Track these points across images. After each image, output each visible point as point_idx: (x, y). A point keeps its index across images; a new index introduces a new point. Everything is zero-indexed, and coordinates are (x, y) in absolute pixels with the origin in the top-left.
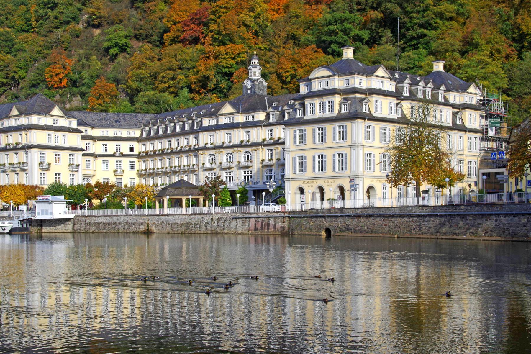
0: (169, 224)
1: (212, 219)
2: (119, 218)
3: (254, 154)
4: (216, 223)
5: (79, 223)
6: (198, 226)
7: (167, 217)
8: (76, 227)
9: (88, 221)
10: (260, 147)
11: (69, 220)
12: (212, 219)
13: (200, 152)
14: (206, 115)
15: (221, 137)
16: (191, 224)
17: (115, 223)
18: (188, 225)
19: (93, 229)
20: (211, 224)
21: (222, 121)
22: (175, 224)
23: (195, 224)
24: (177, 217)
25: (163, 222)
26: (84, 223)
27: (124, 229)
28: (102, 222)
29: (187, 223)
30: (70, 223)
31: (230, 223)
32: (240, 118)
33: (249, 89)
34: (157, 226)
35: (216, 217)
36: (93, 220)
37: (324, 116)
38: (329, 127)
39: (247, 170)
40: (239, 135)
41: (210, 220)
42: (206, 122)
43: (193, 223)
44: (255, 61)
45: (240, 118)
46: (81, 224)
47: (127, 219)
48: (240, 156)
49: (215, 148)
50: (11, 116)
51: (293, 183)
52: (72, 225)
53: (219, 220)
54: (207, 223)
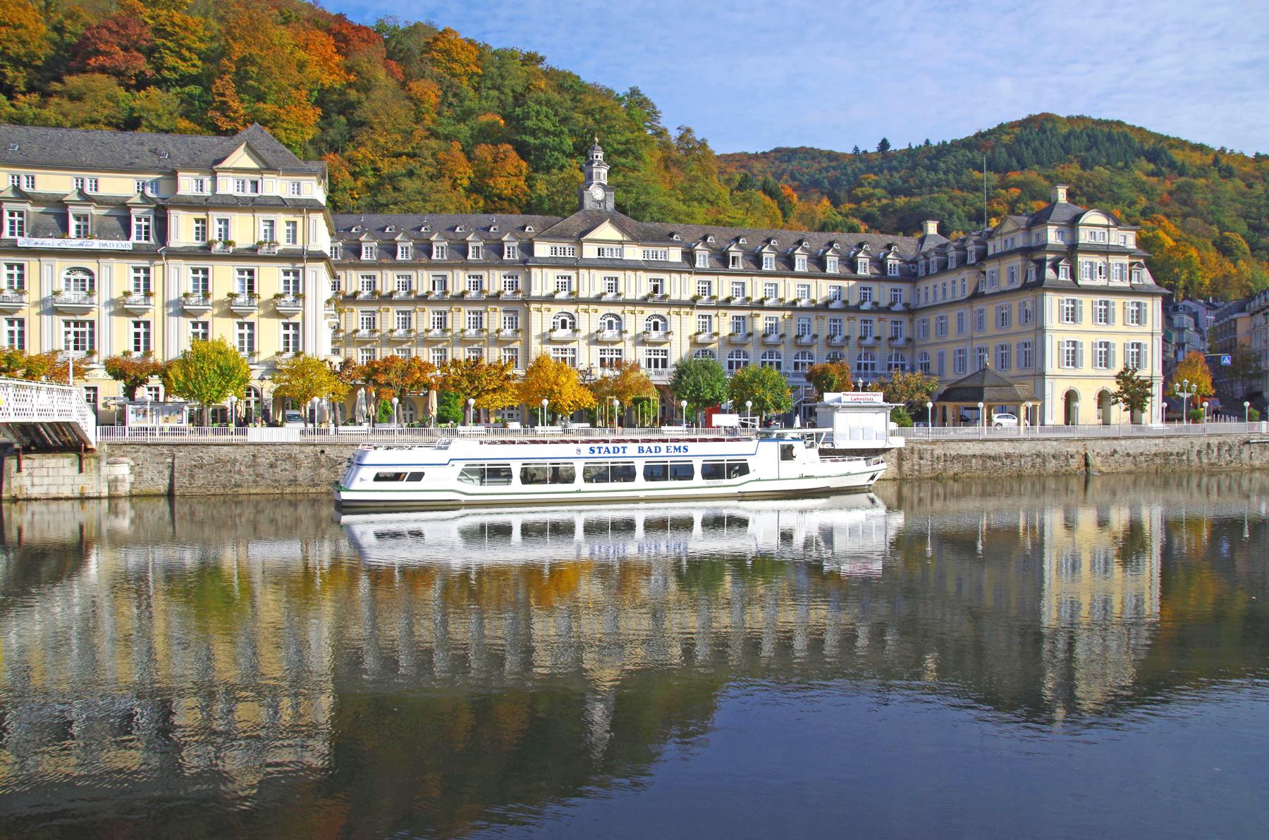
0: (1128, 455)
2: (1017, 444)
3: (674, 323)
5: (916, 456)
6: (1185, 457)
8: (906, 466)
9: (939, 451)
10: (688, 310)
11: (884, 451)
12: (1208, 444)
13: (533, 306)
15: (592, 283)
16: (1171, 454)
17: (1008, 456)
18: (1166, 455)
19: (957, 468)
22: (1141, 454)
25: (1115, 451)
27: (1033, 466)
28: (977, 453)
29: (1165, 454)
30: (887, 456)
31: (1240, 452)
32: (634, 253)
35: (1214, 441)
36: (954, 449)
37: (1111, 284)
38: (1118, 302)
39: (565, 346)
40: (636, 285)
41: (1205, 447)
46: (921, 458)
47: (1040, 447)
48: (636, 322)
51: (1058, 382)
52: (894, 461)
54: (1199, 452)
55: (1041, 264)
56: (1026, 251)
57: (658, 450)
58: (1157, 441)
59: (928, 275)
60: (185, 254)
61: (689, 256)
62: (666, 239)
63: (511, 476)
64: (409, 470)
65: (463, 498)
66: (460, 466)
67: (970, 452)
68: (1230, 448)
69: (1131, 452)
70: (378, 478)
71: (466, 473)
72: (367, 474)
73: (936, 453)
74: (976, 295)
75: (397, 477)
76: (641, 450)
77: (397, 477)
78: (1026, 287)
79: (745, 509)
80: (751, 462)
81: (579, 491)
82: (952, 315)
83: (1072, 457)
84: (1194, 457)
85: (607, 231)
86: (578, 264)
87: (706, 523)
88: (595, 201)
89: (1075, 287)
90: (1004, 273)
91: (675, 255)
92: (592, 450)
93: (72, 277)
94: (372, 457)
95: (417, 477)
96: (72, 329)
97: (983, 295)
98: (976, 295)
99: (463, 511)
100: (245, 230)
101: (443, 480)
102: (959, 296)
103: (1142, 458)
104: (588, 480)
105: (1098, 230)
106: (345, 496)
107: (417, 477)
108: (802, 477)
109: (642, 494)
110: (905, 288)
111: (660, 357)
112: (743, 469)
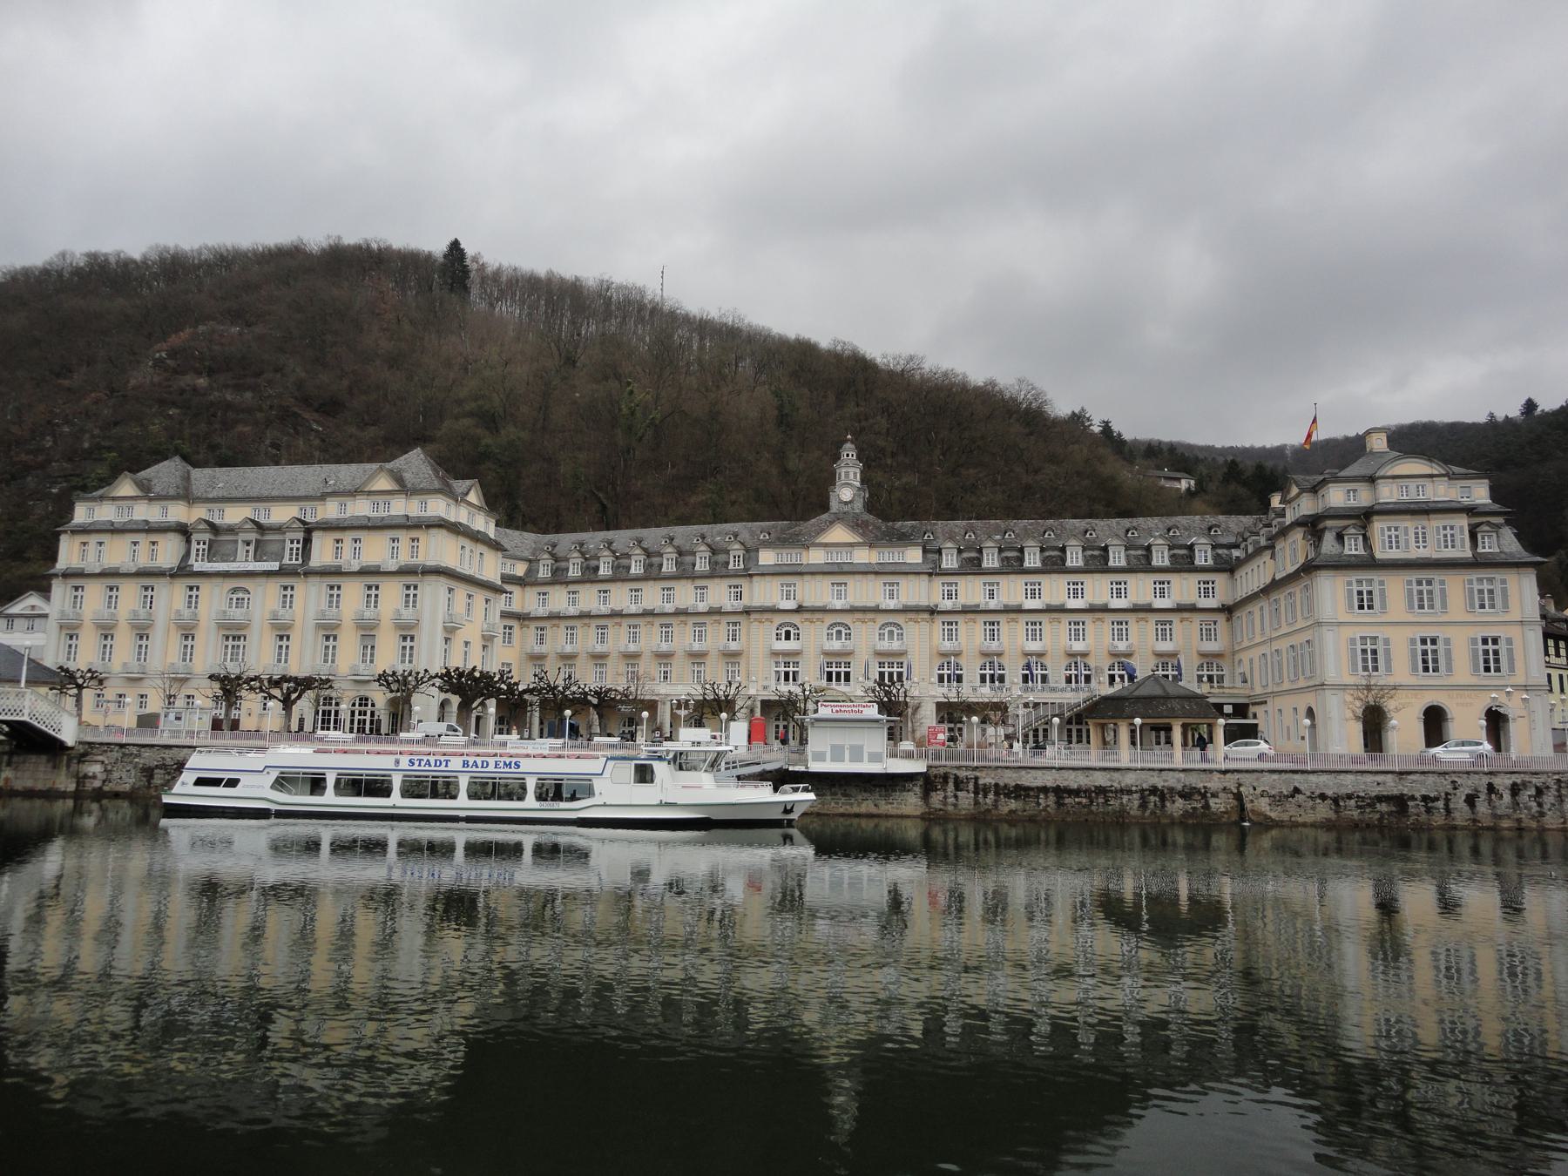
0: (1323, 797)
1: (1491, 788)
4: (1507, 797)
6: (1440, 804)
7: (1312, 778)
11: (910, 777)
14: (767, 545)
15: (816, 592)
16: (1413, 798)
17: (1101, 790)
18: (1400, 801)
20: (1490, 800)
21: (816, 557)
22: (1349, 797)
23: (1425, 798)
24: (1350, 777)
25: (1297, 791)
26: (971, 786)
28: (1049, 784)
32: (863, 556)
33: (846, 503)
34: (1278, 800)
35: (1502, 783)
42: (767, 558)
43: (1417, 795)
44: (849, 453)
45: (863, 556)
53: (1515, 790)
57: (485, 764)
58: (1380, 778)
60: (324, 573)
62: (903, 539)
63: (325, 788)
64: (226, 776)
65: (274, 807)
66: (275, 774)
67: (1039, 783)
68: (1540, 792)
69: (1329, 793)
70: (200, 782)
71: (283, 782)
72: (188, 777)
73: (981, 782)
76: (465, 764)
77: (215, 782)
79: (588, 838)
80: (598, 784)
81: (394, 807)
82: (1255, 608)
83: (1214, 795)
84: (1459, 803)
87: (538, 850)
88: (841, 502)
89: (1370, 563)
92: (412, 762)
93: (235, 597)
94: (194, 761)
95: (233, 783)
96: (230, 643)
99: (273, 820)
100: (376, 550)
101: (257, 790)
103: (1352, 802)
104: (473, 796)
105: (1412, 484)
106: (166, 799)
107: (233, 783)
108: (662, 805)
109: (462, 814)
110: (1220, 580)
111: (843, 669)
112: (590, 792)
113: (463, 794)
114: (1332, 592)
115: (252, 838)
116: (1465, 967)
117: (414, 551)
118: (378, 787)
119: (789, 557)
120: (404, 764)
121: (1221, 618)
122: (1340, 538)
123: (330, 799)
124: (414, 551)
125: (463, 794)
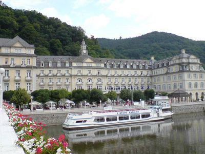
14: (74, 62)
15: (85, 72)
21: (85, 65)
32: (94, 65)
40: (95, 72)
42: (74, 64)
49: (82, 76)
50: (13, 47)
55: (183, 67)
56: (179, 64)
59: (154, 69)
61: (105, 65)
62: (100, 62)
66: (94, 118)
70: (77, 122)
74: (167, 73)
75: (81, 122)
77: (81, 122)
78: (180, 72)
82: (161, 78)
85: (89, 60)
86: (82, 68)
87: (143, 127)
89: (189, 71)
90: (174, 69)
91: (103, 65)
95: (85, 121)
97: (169, 73)
98: (167, 73)
100: (18, 61)
101: (91, 122)
102: (163, 73)
107: (85, 121)
113: (130, 118)
114: (186, 75)
115: (91, 133)
116: (202, 130)
117: (29, 62)
118: (102, 120)
119: (80, 64)
120: (119, 114)
121: (150, 78)
122: (186, 67)
123: (106, 122)
124: (29, 62)
125: (130, 118)
